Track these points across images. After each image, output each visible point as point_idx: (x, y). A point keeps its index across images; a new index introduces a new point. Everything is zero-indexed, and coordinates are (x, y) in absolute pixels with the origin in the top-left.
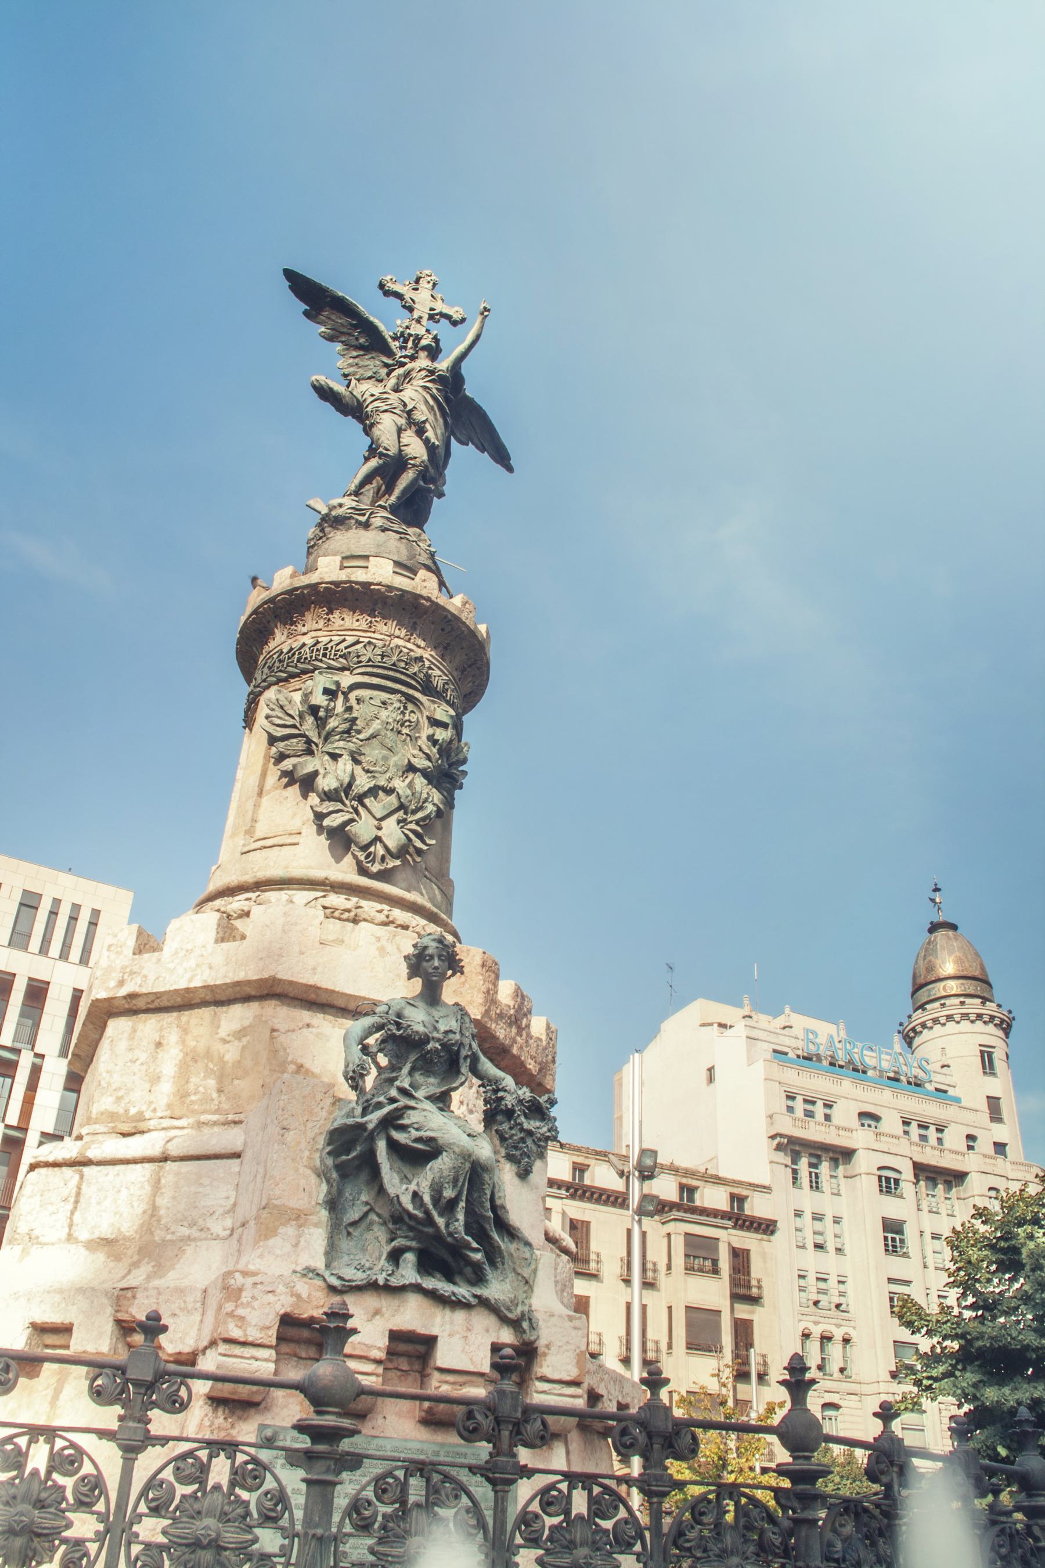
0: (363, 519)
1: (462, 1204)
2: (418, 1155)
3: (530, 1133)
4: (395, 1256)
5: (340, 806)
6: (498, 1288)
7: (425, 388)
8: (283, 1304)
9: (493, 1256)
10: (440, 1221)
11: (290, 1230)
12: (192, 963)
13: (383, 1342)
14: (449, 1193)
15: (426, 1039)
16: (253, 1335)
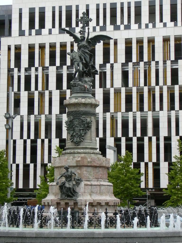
0: (74, 85)
1: (69, 191)
2: (65, 187)
3: (78, 182)
4: (66, 196)
5: (72, 138)
6: (74, 198)
7: (82, 50)
8: (56, 202)
9: (74, 195)
10: (67, 193)
11: (57, 195)
12: (57, 163)
13: (65, 203)
14: (67, 191)
15: (67, 176)
16: (54, 204)
